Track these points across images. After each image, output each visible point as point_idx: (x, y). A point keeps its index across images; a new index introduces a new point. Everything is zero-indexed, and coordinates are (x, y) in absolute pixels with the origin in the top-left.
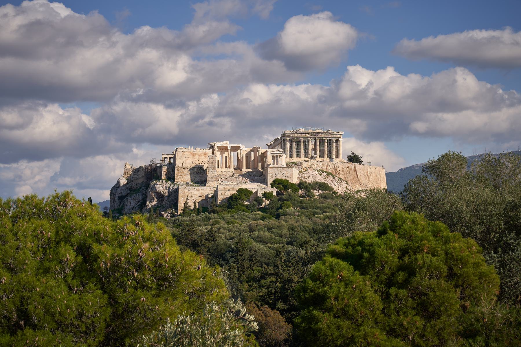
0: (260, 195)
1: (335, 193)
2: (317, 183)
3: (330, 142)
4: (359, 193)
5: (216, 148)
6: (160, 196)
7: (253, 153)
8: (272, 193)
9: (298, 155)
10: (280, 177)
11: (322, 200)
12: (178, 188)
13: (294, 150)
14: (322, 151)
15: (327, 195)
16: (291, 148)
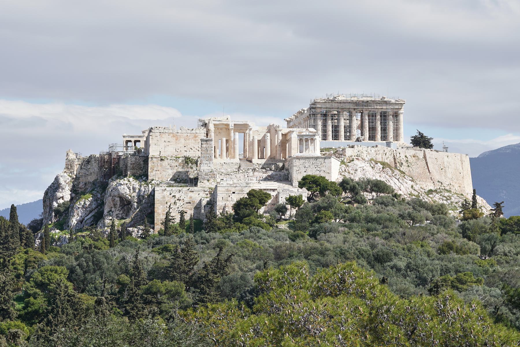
0: (282, 200)
1: (395, 196)
2: (369, 181)
3: (384, 116)
4: (431, 196)
5: (211, 127)
6: (125, 204)
7: (269, 134)
8: (300, 197)
9: (336, 137)
10: (312, 172)
11: (379, 207)
12: (154, 191)
13: (330, 128)
14: (372, 129)
15: (385, 200)
16: (325, 126)
